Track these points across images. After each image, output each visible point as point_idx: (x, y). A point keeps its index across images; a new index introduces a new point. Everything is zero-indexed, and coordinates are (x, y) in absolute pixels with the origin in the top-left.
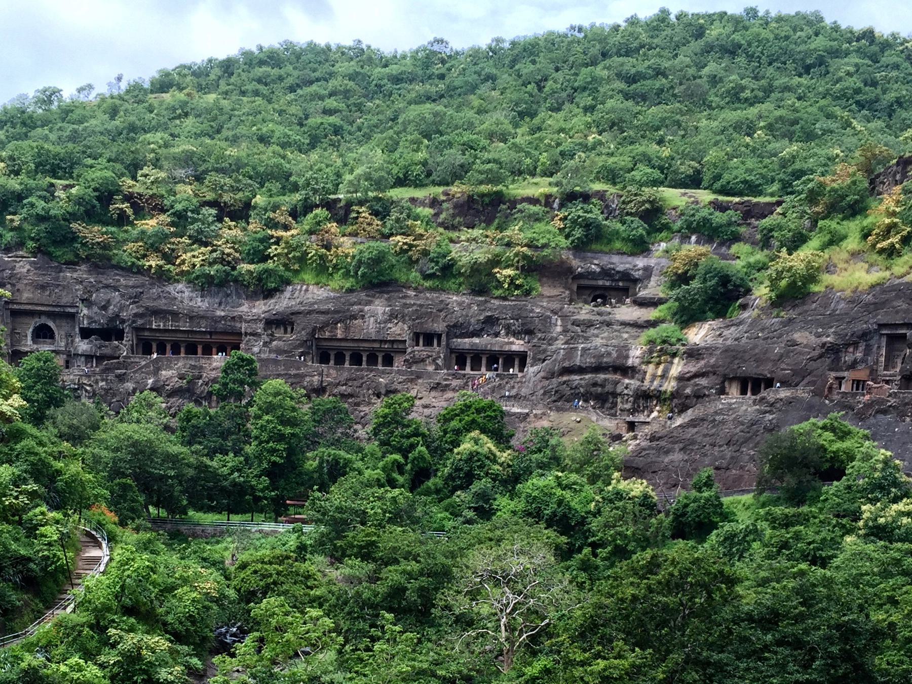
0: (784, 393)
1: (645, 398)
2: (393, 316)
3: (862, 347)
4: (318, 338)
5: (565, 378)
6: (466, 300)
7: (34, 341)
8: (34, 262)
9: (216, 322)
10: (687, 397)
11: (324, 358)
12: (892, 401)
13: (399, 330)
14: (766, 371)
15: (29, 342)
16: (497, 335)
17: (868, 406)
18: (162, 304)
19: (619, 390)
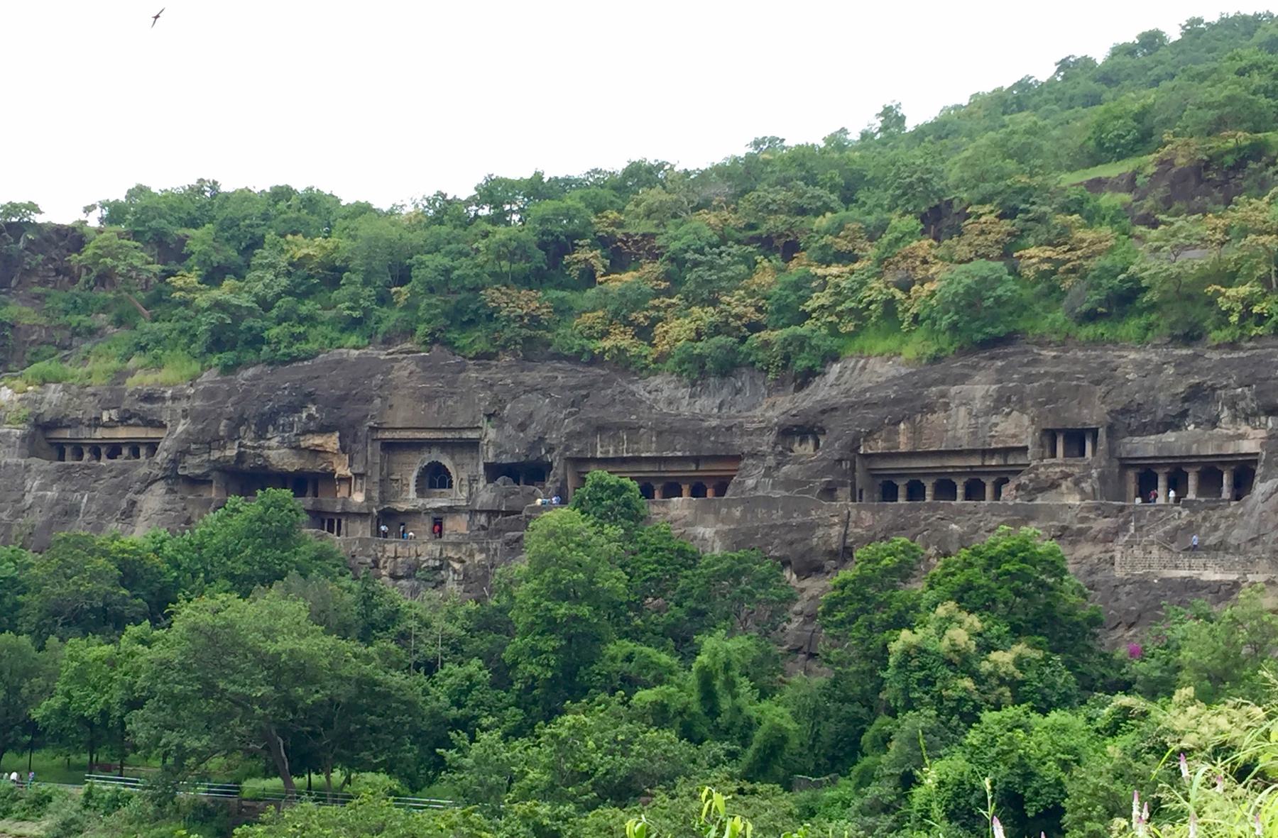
2: (1001, 402)
4: (866, 456)
7: (421, 492)
8: (424, 359)
9: (700, 438)
13: (1016, 428)
15: (412, 494)
18: (612, 415)
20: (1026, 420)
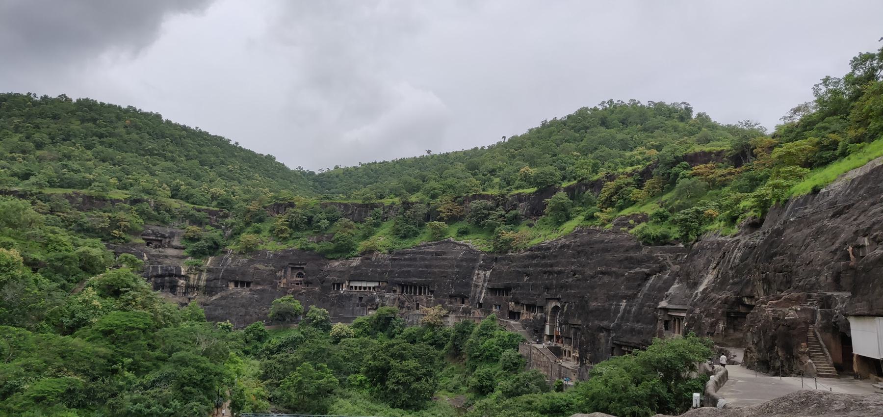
0: (259, 288)
1: (189, 288)
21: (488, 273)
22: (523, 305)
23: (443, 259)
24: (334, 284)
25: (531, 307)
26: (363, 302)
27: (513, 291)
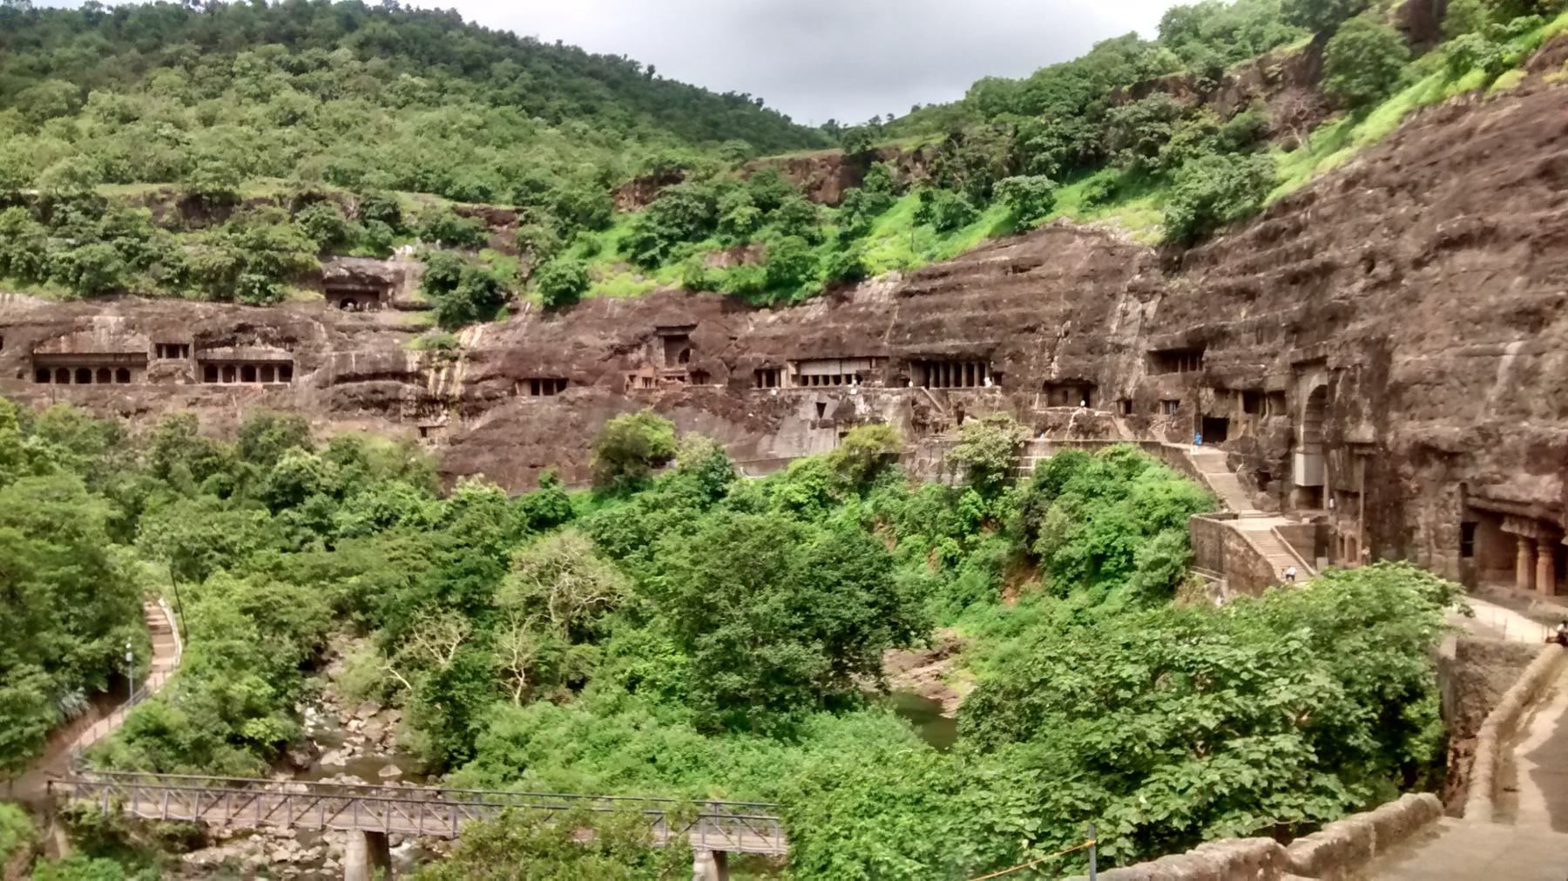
0: (583, 392)
2: (129, 326)
3: (644, 347)
5: (341, 386)
6: (212, 307)
10: (478, 400)
11: (42, 376)
12: (687, 395)
13: (140, 342)
14: (557, 370)
16: (252, 343)
17: (665, 400)
19: (401, 396)
20: (146, 338)
21: (1151, 307)
22: (1236, 392)
23: (1032, 280)
24: (758, 373)
25: (1254, 399)
26: (828, 414)
27: (1208, 353)
